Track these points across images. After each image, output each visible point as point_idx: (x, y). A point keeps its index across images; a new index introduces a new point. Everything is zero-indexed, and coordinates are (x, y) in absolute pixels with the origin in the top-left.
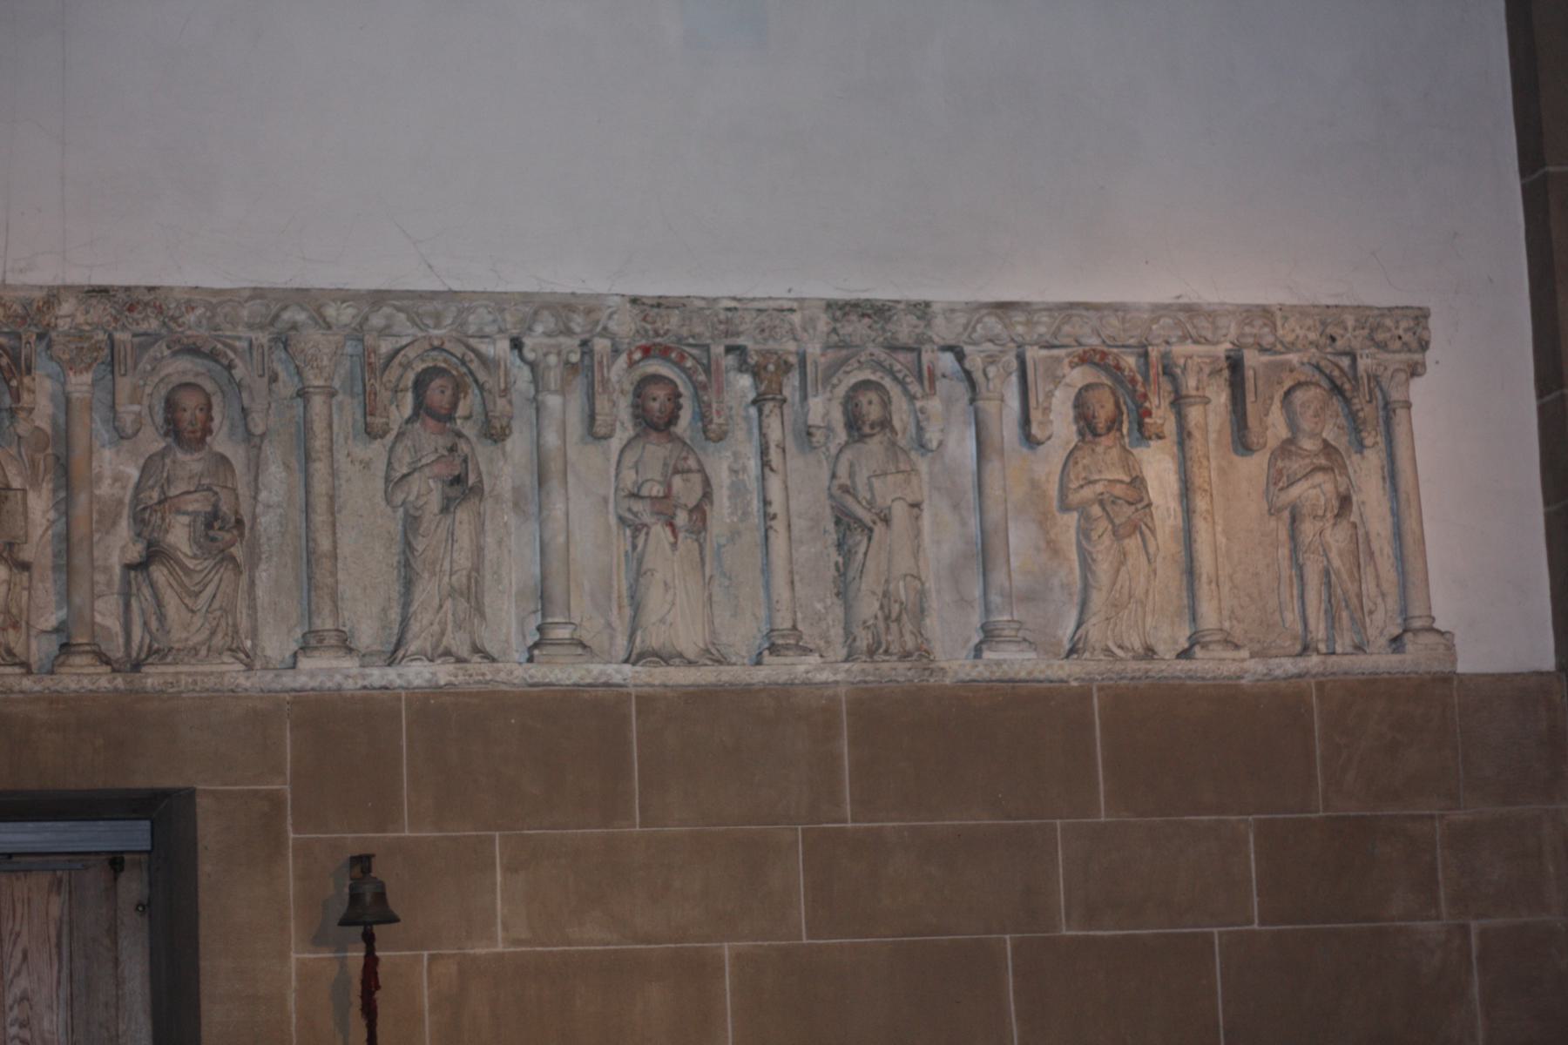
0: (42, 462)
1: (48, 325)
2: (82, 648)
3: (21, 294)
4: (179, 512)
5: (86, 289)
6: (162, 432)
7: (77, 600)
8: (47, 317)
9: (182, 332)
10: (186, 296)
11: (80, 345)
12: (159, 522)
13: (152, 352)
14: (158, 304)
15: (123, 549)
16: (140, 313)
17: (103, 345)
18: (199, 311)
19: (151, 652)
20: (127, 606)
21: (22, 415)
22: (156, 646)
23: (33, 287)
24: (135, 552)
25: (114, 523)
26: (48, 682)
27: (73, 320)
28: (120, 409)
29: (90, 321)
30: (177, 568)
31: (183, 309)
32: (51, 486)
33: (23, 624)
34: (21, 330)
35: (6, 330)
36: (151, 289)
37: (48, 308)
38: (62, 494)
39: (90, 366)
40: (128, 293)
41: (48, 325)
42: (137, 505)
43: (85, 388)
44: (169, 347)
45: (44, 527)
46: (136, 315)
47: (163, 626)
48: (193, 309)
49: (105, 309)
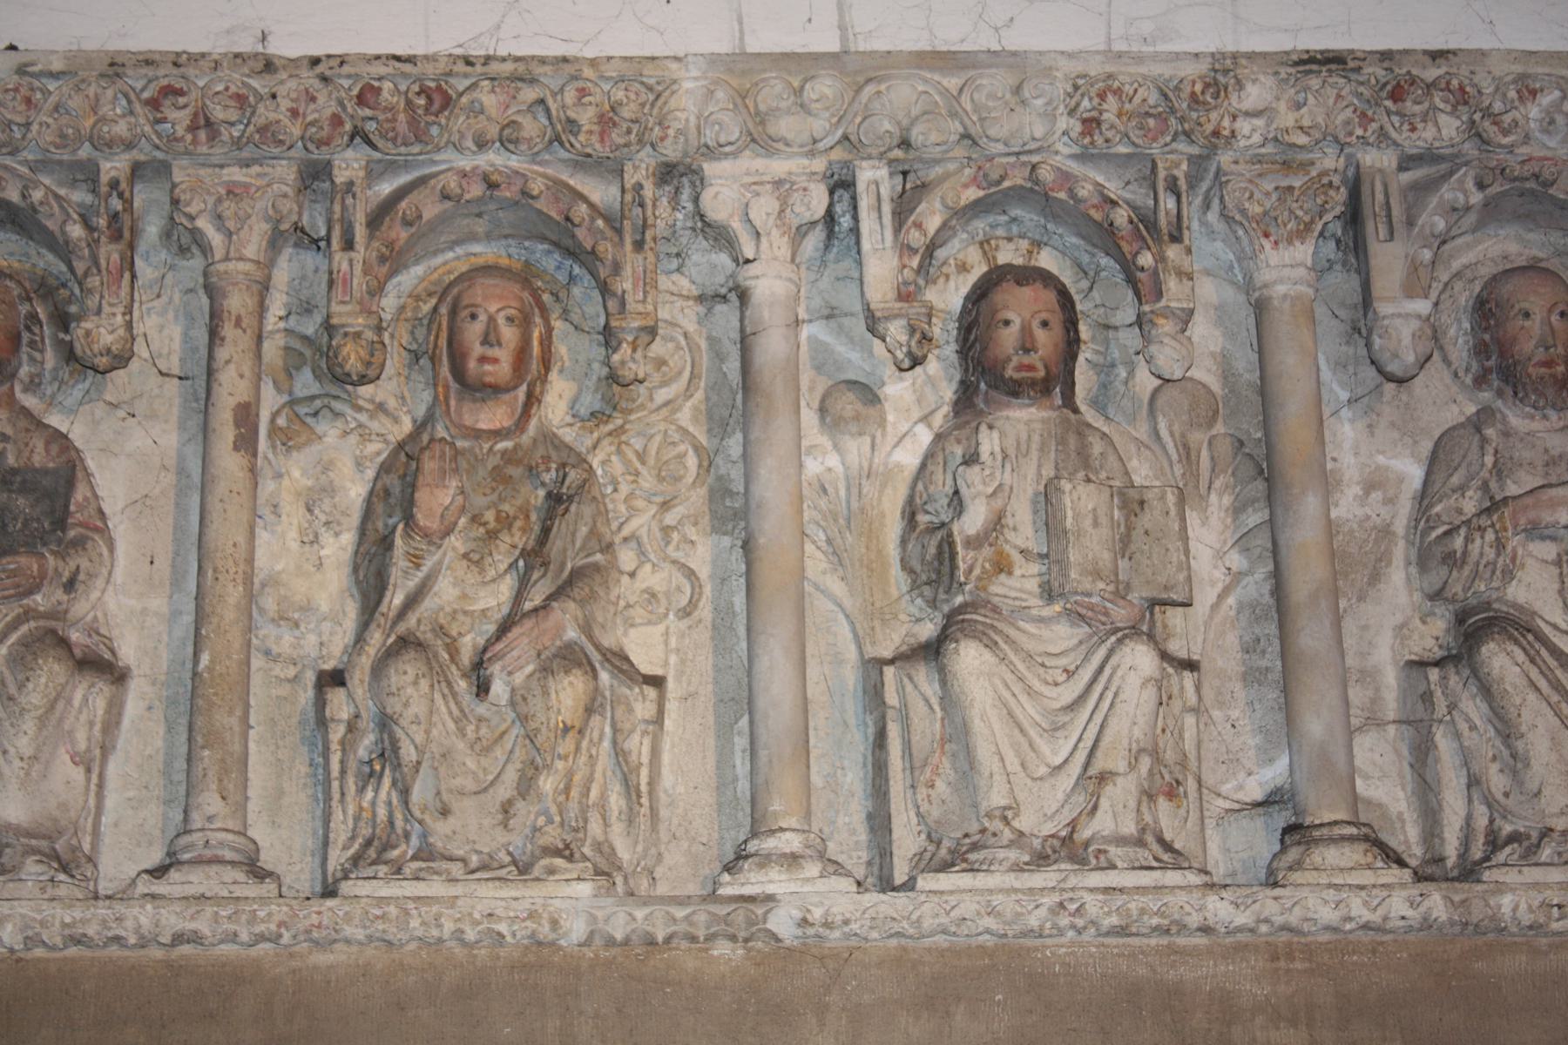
0: (1205, 453)
1: (1216, 133)
2: (1337, 831)
3: (1157, 69)
4: (1535, 531)
5: (1295, 57)
6: (1469, 380)
7: (1316, 725)
8: (1214, 115)
9: (1510, 149)
10: (1518, 68)
11: (1285, 183)
12: (1490, 554)
13: (1447, 193)
14: (1455, 83)
15: (1401, 630)
16: (1416, 103)
17: (1336, 180)
18: (1546, 100)
19: (1494, 843)
20: (1422, 753)
21: (1166, 326)
22: (1508, 829)
23: (1177, 56)
24: (1432, 634)
25: (1375, 578)
26: (1269, 905)
27: (1268, 125)
28: (1384, 308)
29: (1306, 123)
30: (1544, 652)
31: (1512, 94)
32: (1227, 500)
33: (1191, 784)
34: (1155, 151)
35: (1123, 149)
36: (1436, 56)
37: (1216, 96)
38: (1254, 518)
39: (1308, 227)
40: (1386, 64)
41: (1216, 133)
42: (1425, 533)
43: (1301, 272)
44: (1481, 186)
45: (1220, 586)
46: (1409, 106)
47: (1521, 784)
48: (1534, 93)
49: (1339, 96)
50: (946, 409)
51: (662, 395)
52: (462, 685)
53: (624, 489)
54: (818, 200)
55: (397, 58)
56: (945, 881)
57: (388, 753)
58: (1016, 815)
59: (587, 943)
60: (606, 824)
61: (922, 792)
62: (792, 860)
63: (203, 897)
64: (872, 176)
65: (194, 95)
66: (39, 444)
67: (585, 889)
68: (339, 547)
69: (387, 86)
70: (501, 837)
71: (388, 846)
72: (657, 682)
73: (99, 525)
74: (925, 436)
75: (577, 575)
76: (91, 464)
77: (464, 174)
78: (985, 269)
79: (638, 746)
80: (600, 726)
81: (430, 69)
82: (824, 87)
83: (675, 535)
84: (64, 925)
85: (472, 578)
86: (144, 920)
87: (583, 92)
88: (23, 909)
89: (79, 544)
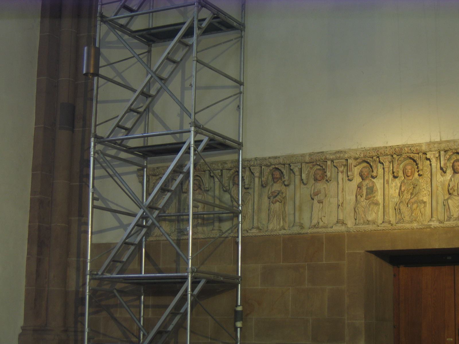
50: (452, 173)
51: (427, 173)
52: (406, 205)
53: (423, 183)
54: (437, 155)
55: (397, 145)
56: (446, 222)
57: (400, 212)
58: (454, 215)
59: (416, 229)
60: (420, 217)
61: (447, 213)
62: (434, 221)
63: (385, 226)
64: (442, 153)
65: (380, 151)
66: (371, 183)
67: (416, 224)
68: (397, 191)
69: (397, 148)
70: (410, 219)
71: (400, 221)
72: (425, 203)
73: (377, 190)
74: (451, 176)
75: (417, 193)
76: (376, 184)
77: (405, 156)
78: (456, 159)
79: (422, 210)
80: (418, 208)
81: (401, 146)
82: (436, 145)
83: (428, 188)
84: (374, 229)
85: (407, 195)
86: (380, 228)
87: (414, 148)
88: (370, 228)
89: (375, 193)
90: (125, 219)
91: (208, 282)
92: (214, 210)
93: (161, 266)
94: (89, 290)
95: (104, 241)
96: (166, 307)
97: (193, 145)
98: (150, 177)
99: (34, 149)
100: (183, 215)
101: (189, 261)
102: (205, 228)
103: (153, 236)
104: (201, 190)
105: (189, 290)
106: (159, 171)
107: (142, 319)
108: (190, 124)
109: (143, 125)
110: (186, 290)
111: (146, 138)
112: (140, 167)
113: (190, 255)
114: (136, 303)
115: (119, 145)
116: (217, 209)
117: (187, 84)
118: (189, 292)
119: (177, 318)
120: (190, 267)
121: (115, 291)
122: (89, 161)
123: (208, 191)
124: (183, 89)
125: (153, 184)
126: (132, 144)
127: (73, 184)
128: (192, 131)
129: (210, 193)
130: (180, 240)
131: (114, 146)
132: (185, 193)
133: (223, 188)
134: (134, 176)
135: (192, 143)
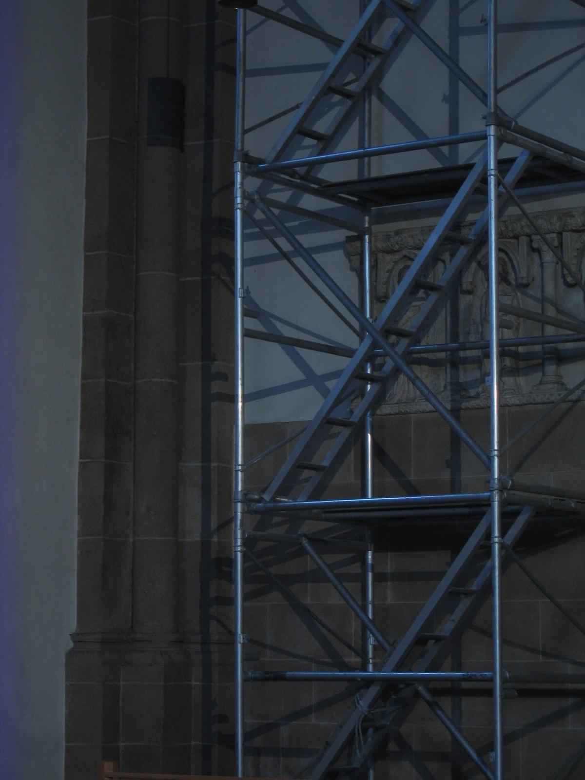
90: (321, 363)
91: (541, 512)
92: (543, 333)
93: (412, 478)
94: (243, 539)
95: (269, 419)
96: (440, 576)
97: (493, 172)
98: (380, 256)
99: (88, 196)
100: (465, 349)
101: (493, 462)
102: (521, 380)
103: (392, 402)
104: (509, 284)
105: (496, 533)
106: (402, 240)
107: (370, 607)
108: (485, 118)
109: (356, 124)
110: (488, 535)
111: (366, 159)
112: (353, 231)
113: (496, 448)
114: (355, 569)
115: (302, 178)
116: (550, 331)
117: (468, 19)
118: (496, 540)
119: (464, 605)
120: (496, 476)
121: (305, 542)
122: (232, 224)
123: (526, 286)
124: (455, 32)
125: (388, 274)
126: (332, 173)
127: (187, 279)
128: (490, 135)
129: (531, 292)
130: (459, 410)
131: (289, 180)
132: (469, 292)
133: (563, 276)
134: (339, 254)
135: (492, 165)
